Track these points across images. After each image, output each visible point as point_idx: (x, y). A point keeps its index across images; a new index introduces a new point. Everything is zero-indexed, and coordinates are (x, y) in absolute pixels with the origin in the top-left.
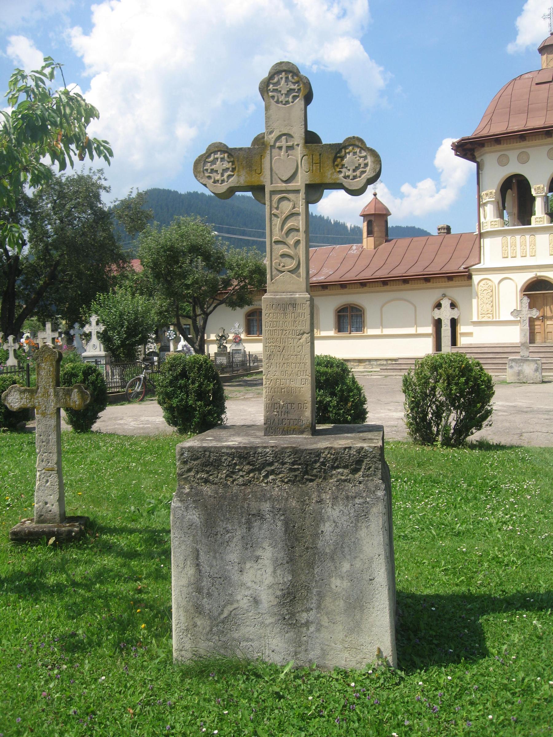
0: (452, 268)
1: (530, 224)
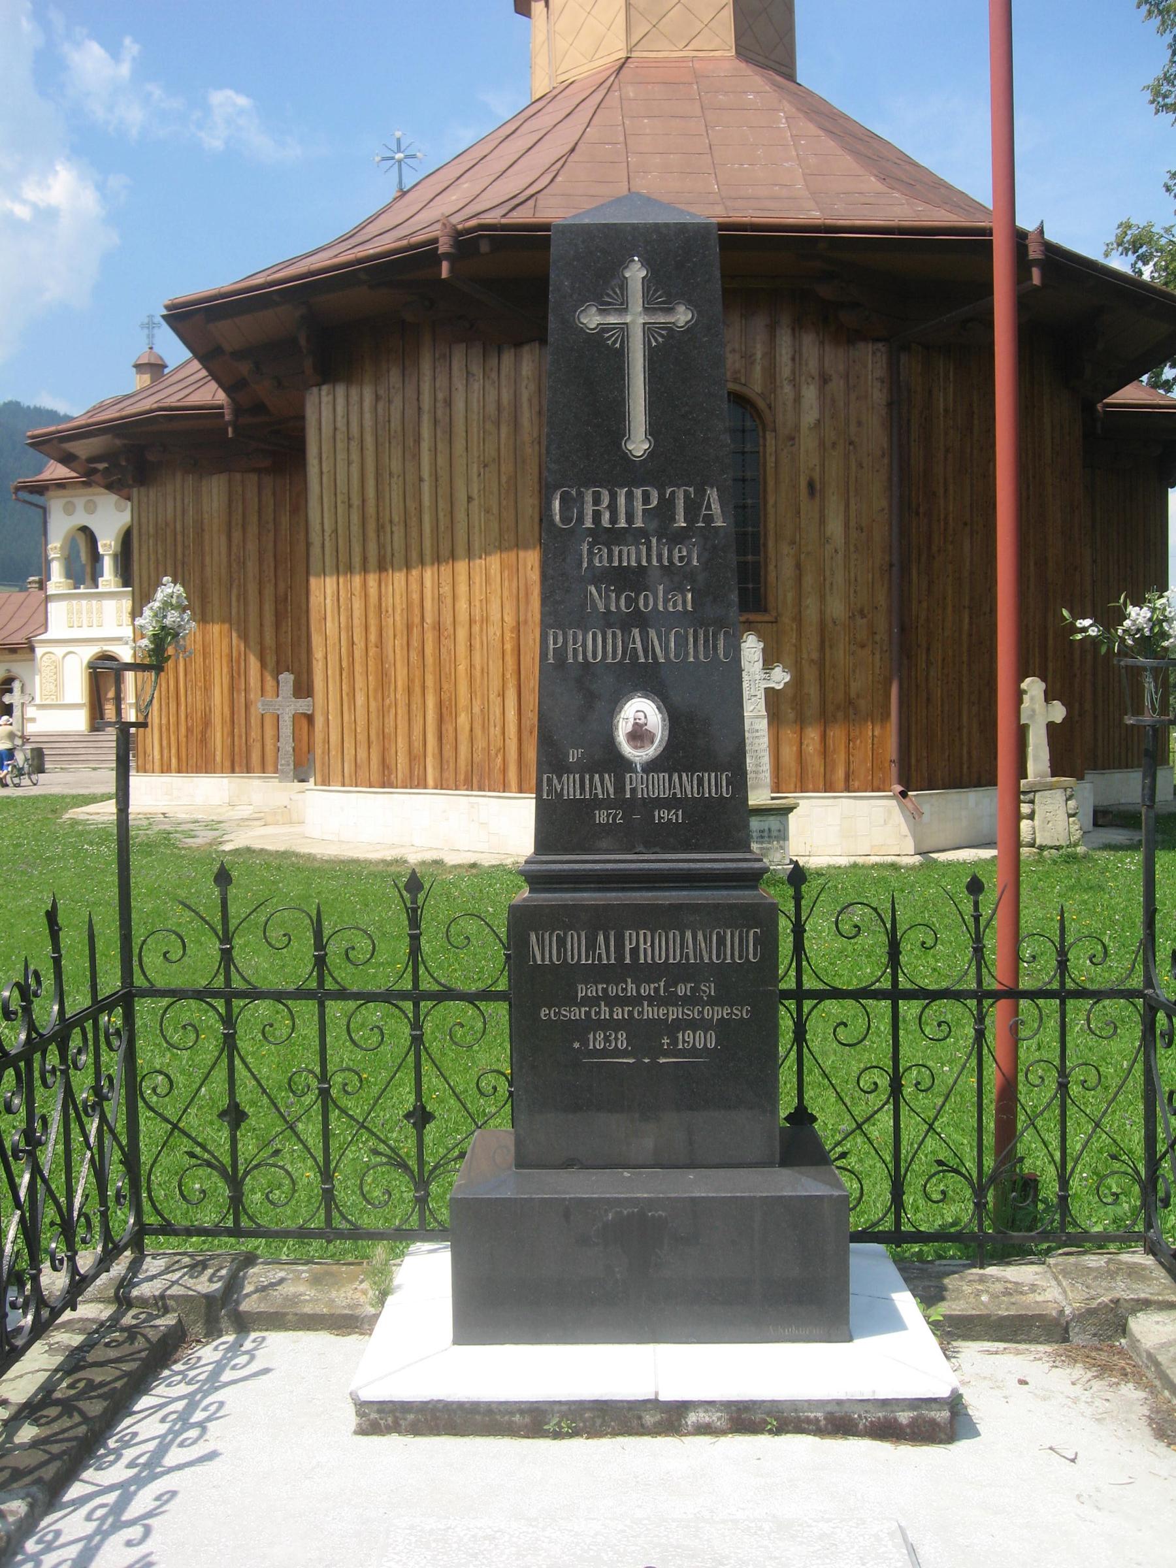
0: (18, 638)
1: (97, 587)
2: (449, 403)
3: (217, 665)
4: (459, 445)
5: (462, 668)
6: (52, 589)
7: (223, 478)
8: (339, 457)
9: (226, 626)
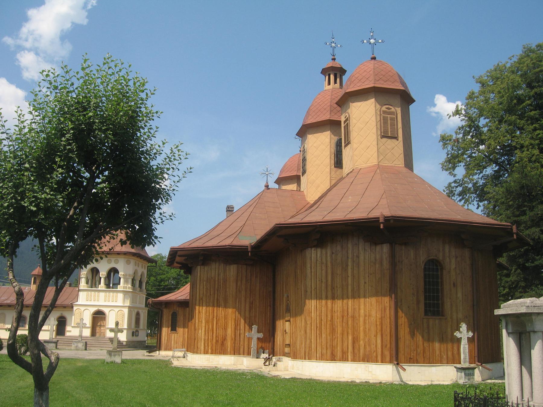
0: (66, 303)
2: (358, 257)
3: (230, 322)
4: (362, 268)
5: (362, 328)
6: (81, 288)
7: (235, 266)
8: (318, 268)
9: (235, 310)
